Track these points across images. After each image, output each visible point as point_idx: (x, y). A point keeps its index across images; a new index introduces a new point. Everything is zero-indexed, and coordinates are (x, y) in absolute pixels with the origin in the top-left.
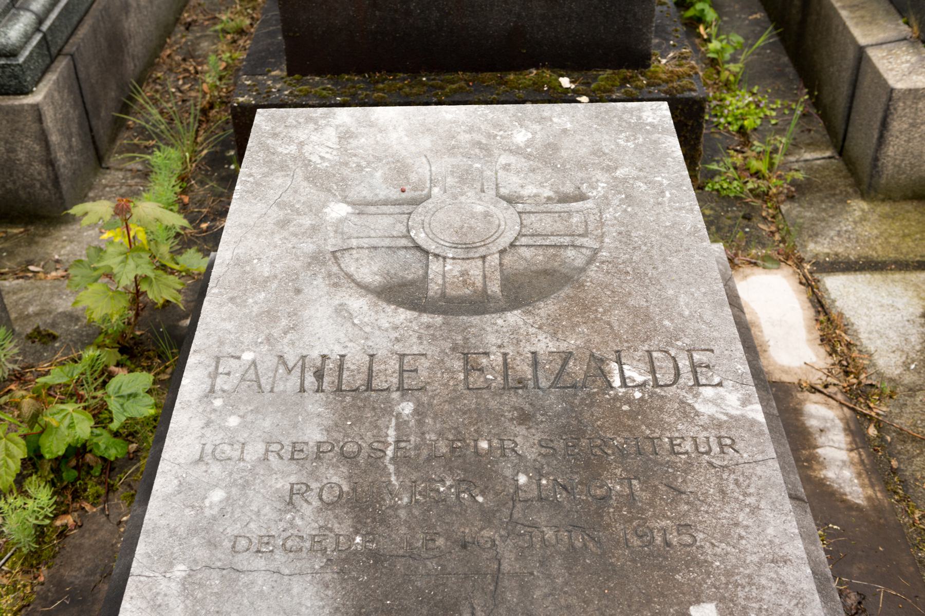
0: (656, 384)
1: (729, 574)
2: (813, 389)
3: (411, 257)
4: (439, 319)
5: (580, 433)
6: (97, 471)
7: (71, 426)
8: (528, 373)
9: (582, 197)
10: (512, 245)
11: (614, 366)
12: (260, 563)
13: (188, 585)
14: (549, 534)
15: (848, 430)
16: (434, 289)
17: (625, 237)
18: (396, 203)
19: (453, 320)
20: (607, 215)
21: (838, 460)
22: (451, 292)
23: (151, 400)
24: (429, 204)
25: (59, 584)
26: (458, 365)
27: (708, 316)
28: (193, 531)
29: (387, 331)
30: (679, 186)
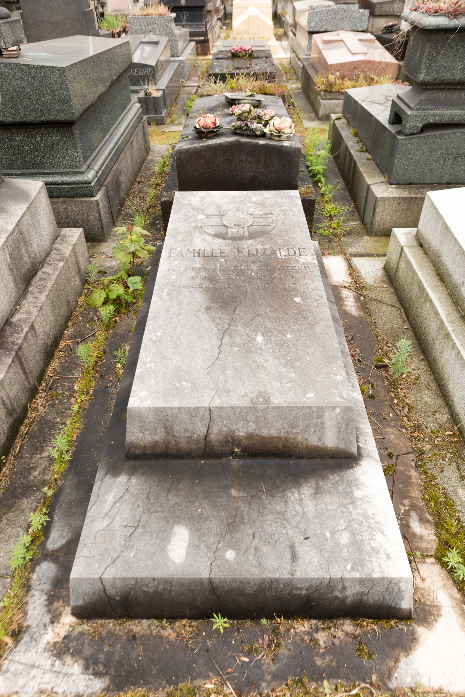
0: (289, 255)
1: (304, 292)
2: (345, 287)
3: (223, 228)
4: (231, 241)
5: (268, 265)
6: (124, 306)
7: (118, 290)
8: (255, 253)
9: (272, 214)
10: (251, 225)
11: (278, 252)
12: (187, 290)
13: (168, 294)
14: (259, 285)
15: (355, 298)
16: (229, 235)
17: (283, 223)
18: (218, 215)
19: (234, 242)
20: (278, 218)
21: (350, 305)
22: (234, 236)
23: (141, 284)
24: (228, 215)
25: (116, 334)
26: (236, 251)
27: (305, 241)
28: (168, 284)
29: (217, 244)
30: (300, 211)
